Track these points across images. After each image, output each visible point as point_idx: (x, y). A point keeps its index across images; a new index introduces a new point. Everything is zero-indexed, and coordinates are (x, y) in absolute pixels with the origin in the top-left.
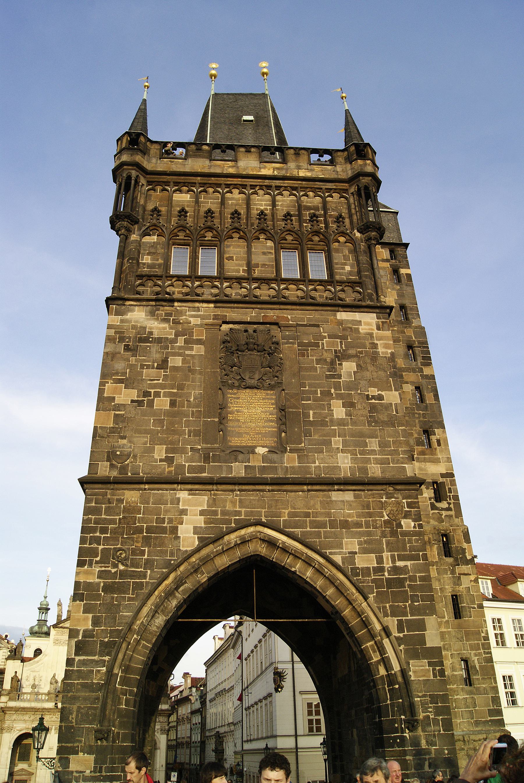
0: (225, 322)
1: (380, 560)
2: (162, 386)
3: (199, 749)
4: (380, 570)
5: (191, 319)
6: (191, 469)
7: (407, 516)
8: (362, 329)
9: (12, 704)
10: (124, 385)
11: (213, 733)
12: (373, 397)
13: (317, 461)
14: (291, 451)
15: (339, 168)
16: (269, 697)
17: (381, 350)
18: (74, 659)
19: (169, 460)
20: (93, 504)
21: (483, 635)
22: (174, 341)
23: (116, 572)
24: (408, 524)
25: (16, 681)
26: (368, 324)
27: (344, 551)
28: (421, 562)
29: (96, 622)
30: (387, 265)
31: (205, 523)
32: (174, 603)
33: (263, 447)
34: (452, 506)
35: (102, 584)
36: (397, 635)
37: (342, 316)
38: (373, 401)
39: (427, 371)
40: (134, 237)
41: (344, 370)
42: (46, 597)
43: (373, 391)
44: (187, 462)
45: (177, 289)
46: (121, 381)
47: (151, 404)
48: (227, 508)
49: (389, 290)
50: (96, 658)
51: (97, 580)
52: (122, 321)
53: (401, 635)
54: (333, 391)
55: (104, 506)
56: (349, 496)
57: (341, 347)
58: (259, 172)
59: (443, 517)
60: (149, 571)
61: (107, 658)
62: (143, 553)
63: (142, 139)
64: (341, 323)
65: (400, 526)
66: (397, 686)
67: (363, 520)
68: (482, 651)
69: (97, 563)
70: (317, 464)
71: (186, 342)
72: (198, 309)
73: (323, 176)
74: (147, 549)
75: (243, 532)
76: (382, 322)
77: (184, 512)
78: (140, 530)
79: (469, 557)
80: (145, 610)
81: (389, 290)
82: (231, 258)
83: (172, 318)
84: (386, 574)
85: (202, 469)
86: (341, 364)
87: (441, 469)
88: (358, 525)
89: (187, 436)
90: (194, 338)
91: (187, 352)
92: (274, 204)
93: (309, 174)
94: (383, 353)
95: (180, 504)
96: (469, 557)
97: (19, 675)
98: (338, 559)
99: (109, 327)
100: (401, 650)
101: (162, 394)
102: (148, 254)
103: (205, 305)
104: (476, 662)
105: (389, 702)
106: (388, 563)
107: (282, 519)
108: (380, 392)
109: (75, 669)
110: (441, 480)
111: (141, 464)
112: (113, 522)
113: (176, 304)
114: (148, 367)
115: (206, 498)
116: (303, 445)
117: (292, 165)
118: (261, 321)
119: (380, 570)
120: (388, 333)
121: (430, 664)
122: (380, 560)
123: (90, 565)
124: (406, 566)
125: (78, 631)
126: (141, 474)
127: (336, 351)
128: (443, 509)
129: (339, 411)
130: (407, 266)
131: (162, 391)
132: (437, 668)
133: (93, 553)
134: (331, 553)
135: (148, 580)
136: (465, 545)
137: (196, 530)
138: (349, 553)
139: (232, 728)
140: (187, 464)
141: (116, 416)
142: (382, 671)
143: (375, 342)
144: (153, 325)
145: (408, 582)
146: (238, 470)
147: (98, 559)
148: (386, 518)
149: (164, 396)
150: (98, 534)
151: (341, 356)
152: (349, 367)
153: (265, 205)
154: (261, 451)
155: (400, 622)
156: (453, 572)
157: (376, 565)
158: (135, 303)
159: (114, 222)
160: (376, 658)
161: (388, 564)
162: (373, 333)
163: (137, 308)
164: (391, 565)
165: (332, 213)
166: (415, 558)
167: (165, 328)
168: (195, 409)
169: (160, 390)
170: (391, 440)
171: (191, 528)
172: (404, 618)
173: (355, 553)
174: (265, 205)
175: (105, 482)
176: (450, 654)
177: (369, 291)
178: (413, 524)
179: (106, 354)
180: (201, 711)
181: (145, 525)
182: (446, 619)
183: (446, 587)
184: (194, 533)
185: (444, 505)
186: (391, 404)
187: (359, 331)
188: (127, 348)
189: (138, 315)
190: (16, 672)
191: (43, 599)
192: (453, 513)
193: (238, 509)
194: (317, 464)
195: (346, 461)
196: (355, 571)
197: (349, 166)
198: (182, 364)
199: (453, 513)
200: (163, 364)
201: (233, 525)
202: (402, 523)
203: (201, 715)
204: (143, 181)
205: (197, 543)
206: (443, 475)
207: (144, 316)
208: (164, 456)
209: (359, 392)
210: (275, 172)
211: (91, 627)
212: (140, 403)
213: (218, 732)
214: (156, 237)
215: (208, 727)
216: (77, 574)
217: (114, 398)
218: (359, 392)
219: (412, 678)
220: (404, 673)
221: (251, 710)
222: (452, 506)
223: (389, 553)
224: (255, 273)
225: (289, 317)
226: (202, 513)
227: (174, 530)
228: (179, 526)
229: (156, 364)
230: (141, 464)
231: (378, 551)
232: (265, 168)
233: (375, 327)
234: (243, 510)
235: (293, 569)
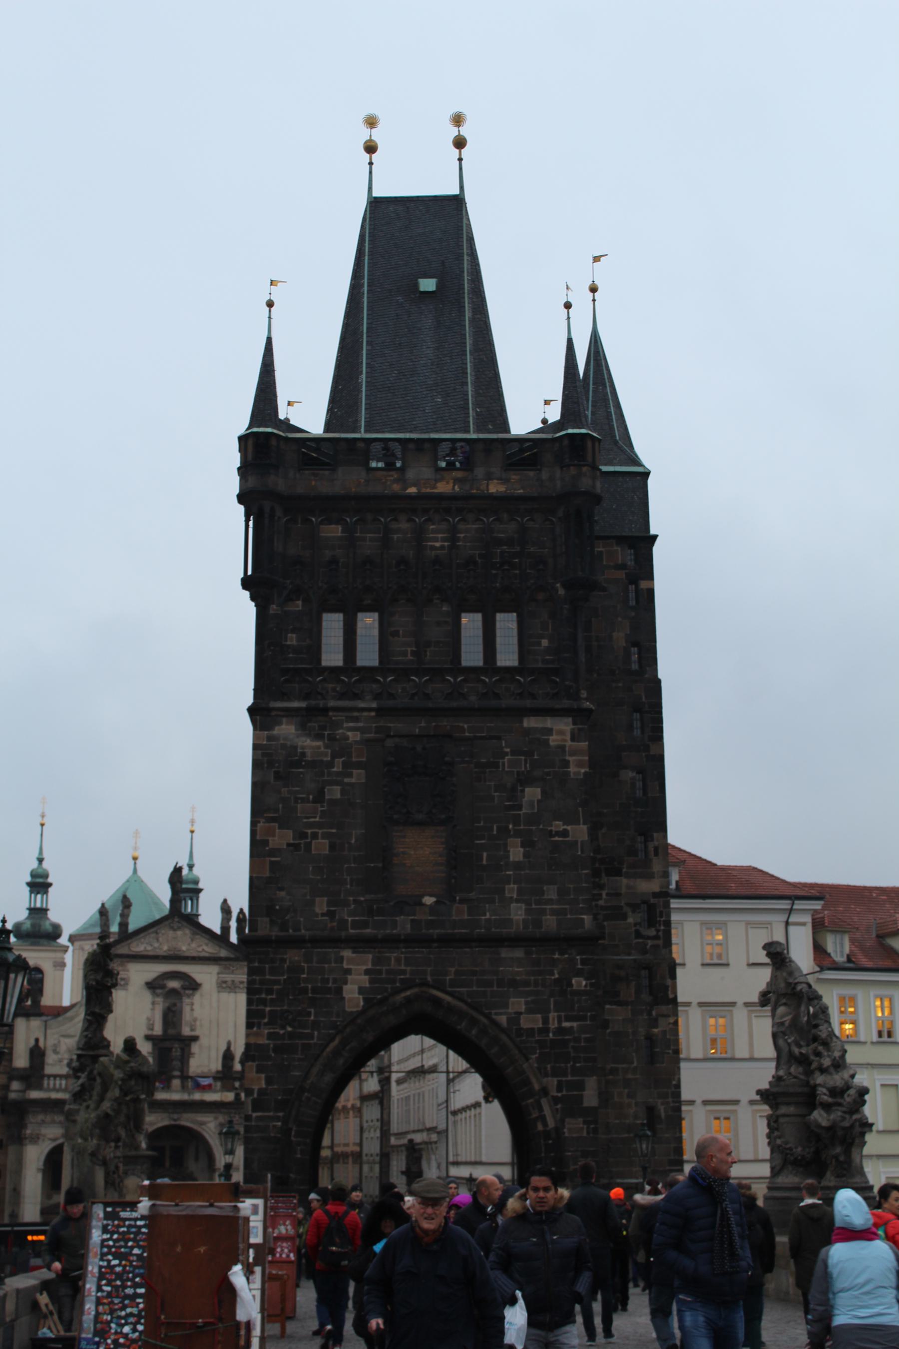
0: (389, 736)
1: (546, 1021)
2: (319, 825)
3: (377, 1168)
4: (545, 1030)
5: (350, 734)
6: (355, 925)
7: (579, 973)
8: (553, 741)
9: (35, 1095)
10: (276, 825)
11: (405, 1141)
12: (558, 834)
13: (488, 914)
14: (462, 901)
15: (545, 475)
16: (475, 1108)
17: (572, 769)
18: (251, 1116)
19: (331, 914)
20: (256, 964)
21: (674, 1083)
22: (331, 764)
23: (284, 1034)
24: (579, 983)
25: (37, 1054)
26: (561, 732)
27: (510, 1010)
28: (588, 1022)
29: (269, 1081)
30: (621, 575)
31: (370, 982)
32: (341, 1061)
33: (431, 895)
34: (661, 934)
35: (272, 1046)
36: (555, 1094)
37: (530, 722)
38: (557, 838)
39: (653, 751)
40: (273, 609)
41: (526, 799)
42: (41, 860)
43: (558, 825)
44: (349, 916)
45: (330, 686)
46: (273, 820)
47: (308, 847)
48: (392, 967)
49: (620, 619)
50: (271, 1114)
51: (267, 1042)
52: (269, 738)
53: (560, 1095)
54: (511, 826)
55: (267, 966)
56: (519, 953)
57: (526, 767)
58: (435, 488)
59: (648, 947)
60: (316, 1033)
61: (281, 1114)
62: (309, 1014)
63: (274, 442)
64: (528, 732)
65: (572, 985)
66: (550, 1142)
67: (532, 978)
68: (670, 1100)
69: (265, 1024)
70: (488, 916)
71: (345, 765)
72: (356, 719)
73: (521, 491)
74: (312, 1010)
75: (408, 993)
76: (579, 729)
77: (348, 972)
78: (304, 991)
79: (671, 996)
80: (315, 1070)
81: (620, 619)
82: (396, 634)
83: (326, 733)
84: (551, 1035)
85: (365, 925)
86: (523, 791)
87: (654, 886)
88: (527, 983)
89: (349, 886)
90: (354, 760)
91: (346, 780)
92: (453, 539)
93: (502, 489)
94: (575, 773)
95: (345, 962)
96: (671, 996)
97: (41, 1044)
98: (503, 1020)
99: (255, 747)
100: (557, 1109)
101: (320, 836)
102: (293, 631)
103: (365, 714)
104: (662, 1111)
105: (543, 1155)
106: (553, 1024)
107: (448, 978)
108: (565, 827)
109: (253, 1123)
110: (652, 901)
111: (302, 919)
112: (277, 982)
113: (331, 714)
114: (303, 800)
115: (370, 956)
116: (474, 893)
117: (479, 472)
118: (432, 733)
119: (545, 1030)
120: (584, 745)
121: (585, 1122)
122: (546, 1021)
123: (259, 1027)
124: (572, 1027)
125: (253, 1090)
126: (303, 931)
127: (518, 773)
128: (649, 938)
129: (516, 853)
130: (650, 576)
131: (320, 831)
132: (592, 1126)
133: (261, 1014)
134: (496, 1014)
135: (315, 1041)
136: (669, 982)
137: (361, 990)
138: (515, 1013)
139: (434, 1137)
140: (350, 919)
141: (272, 863)
142: (540, 1127)
143: (567, 758)
144: (305, 744)
145: (572, 1044)
146: (403, 925)
147: (266, 1020)
148: (557, 976)
149: (323, 838)
150: (263, 996)
151: (525, 780)
152: (533, 793)
153: (443, 540)
154: (429, 900)
155: (559, 1082)
156: (650, 1014)
157: (541, 1026)
158: (282, 713)
159: (246, 583)
160: (535, 1114)
161: (553, 1025)
162: (565, 746)
163: (284, 720)
164: (556, 1025)
165: (532, 549)
166: (584, 1018)
167: (319, 747)
168: (356, 854)
169: (316, 830)
170: (572, 886)
171: (356, 987)
172: (564, 1079)
173: (521, 1013)
174: (443, 540)
175: (266, 941)
176: (634, 1101)
177: (567, 683)
178: (584, 983)
179: (254, 785)
180: (382, 1097)
181: (310, 986)
182: (635, 1064)
183: (641, 1030)
184: (360, 993)
185: (652, 932)
186: (576, 842)
187: (549, 745)
188: (277, 776)
189: (286, 730)
190: (37, 1040)
191: (35, 864)
192: (660, 942)
193: (403, 967)
194: (488, 916)
195: (519, 913)
196: (520, 1031)
197: (558, 473)
198: (342, 794)
199: (660, 942)
200: (319, 797)
201: (398, 985)
202: (574, 981)
203: (381, 1103)
204: (279, 513)
205: (362, 1003)
206: (655, 895)
207: (293, 731)
208: (325, 909)
209: (541, 827)
210: (456, 487)
211: (264, 1086)
212: (296, 847)
213: (411, 1141)
214: (300, 603)
215: (395, 1127)
216: (248, 1035)
217: (268, 841)
218: (541, 827)
219: (566, 1135)
220: (558, 1130)
221: (459, 1116)
222: (661, 934)
223: (556, 1014)
224: (426, 656)
225: (466, 726)
226: (367, 972)
227: (339, 991)
228: (345, 988)
229: (311, 797)
230: (302, 919)
231: (545, 1012)
232: (442, 479)
233: (568, 737)
234: (408, 969)
235: (459, 1027)
